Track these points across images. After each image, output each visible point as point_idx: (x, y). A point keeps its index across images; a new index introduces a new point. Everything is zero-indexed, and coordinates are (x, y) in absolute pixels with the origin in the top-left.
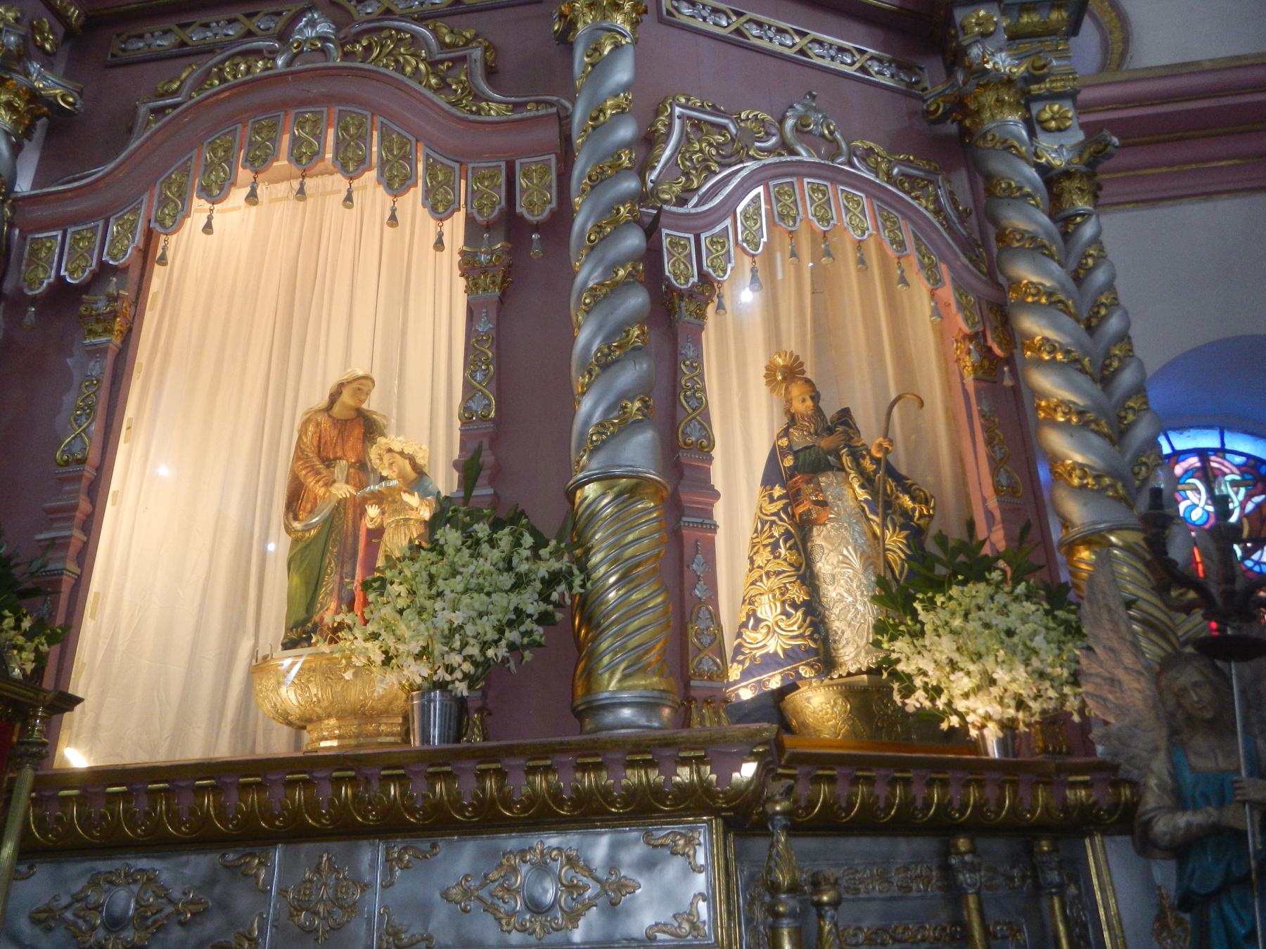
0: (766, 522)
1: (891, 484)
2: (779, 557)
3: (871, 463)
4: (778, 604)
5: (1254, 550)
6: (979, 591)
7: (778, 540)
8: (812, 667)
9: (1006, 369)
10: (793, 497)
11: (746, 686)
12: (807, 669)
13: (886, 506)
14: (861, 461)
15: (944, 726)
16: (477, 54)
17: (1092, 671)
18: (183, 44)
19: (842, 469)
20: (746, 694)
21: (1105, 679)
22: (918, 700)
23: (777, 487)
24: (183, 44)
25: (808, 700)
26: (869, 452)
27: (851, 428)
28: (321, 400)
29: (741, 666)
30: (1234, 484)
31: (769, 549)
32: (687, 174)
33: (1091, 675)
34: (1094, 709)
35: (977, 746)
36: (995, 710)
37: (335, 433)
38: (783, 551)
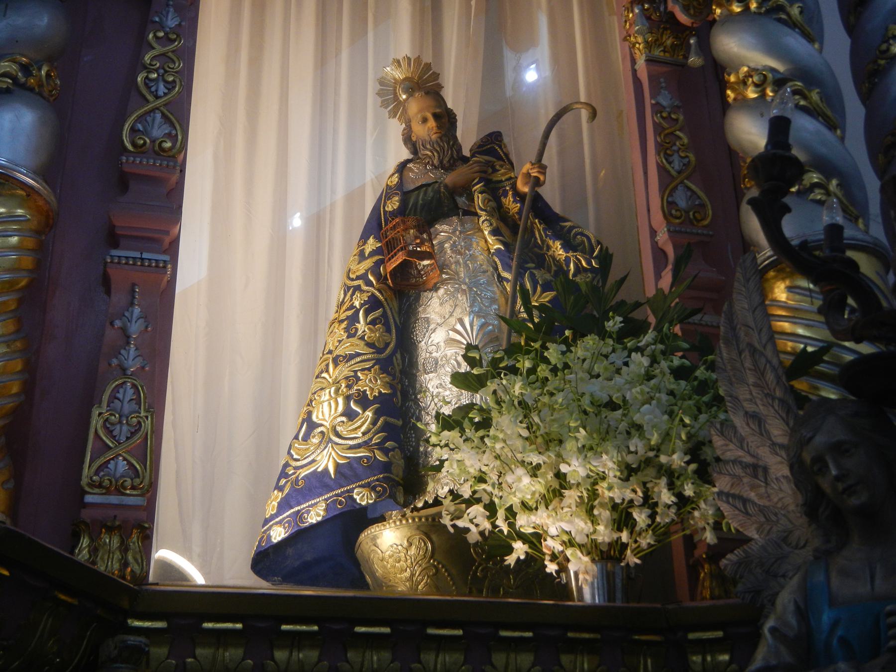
0: (349, 288)
2: (353, 335)
3: (515, 201)
4: (341, 400)
7: (358, 311)
8: (373, 489)
9: (692, 41)
11: (280, 523)
12: (365, 491)
14: (503, 200)
15: (511, 560)
17: (729, 455)
20: (278, 534)
21: (745, 466)
23: (371, 240)
25: (374, 539)
26: (514, 187)
27: (500, 158)
29: (280, 494)
31: (344, 325)
33: (726, 462)
34: (734, 522)
36: (580, 526)
38: (362, 326)
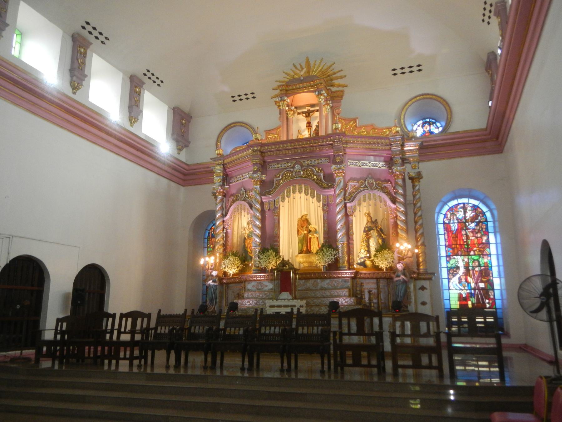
1: (381, 232)
5: (470, 224)
6: (385, 252)
10: (367, 235)
13: (379, 236)
16: (322, 174)
18: (278, 167)
19: (374, 230)
20: (359, 262)
22: (377, 264)
24: (278, 167)
28: (300, 217)
30: (469, 210)
32: (351, 194)
35: (383, 270)
36: (384, 266)
37: (303, 223)
38: (365, 243)
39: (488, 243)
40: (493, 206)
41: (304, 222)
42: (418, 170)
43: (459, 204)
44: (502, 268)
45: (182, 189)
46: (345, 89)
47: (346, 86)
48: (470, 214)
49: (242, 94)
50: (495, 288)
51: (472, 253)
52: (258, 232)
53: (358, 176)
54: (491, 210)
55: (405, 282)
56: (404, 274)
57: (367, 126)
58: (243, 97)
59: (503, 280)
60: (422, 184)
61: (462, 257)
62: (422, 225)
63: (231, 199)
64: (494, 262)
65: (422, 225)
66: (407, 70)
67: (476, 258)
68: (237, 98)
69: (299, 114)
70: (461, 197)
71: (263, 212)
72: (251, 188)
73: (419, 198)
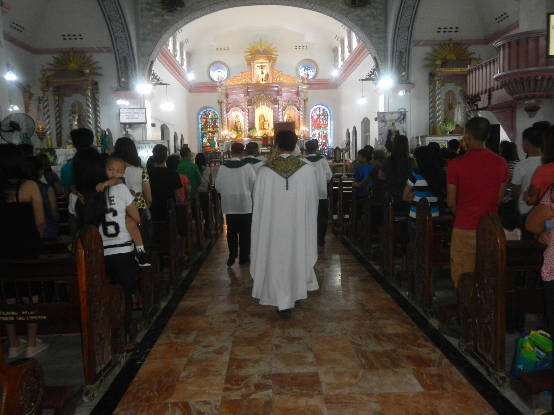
16: (273, 98)
28: (260, 114)
39: (327, 124)
40: (330, 109)
41: (262, 116)
42: (307, 97)
43: (317, 108)
44: (332, 135)
45: (190, 94)
46: (277, 57)
47: (278, 56)
48: (322, 112)
49: (223, 47)
50: (329, 142)
51: (321, 128)
52: (247, 121)
53: (286, 100)
54: (329, 111)
55: (303, 141)
56: (303, 138)
57: (286, 75)
58: (223, 49)
59: (332, 139)
60: (308, 103)
61: (318, 130)
62: (307, 119)
63: (230, 105)
64: (329, 132)
65: (307, 119)
66: (301, 47)
67: (323, 130)
68: (219, 49)
69: (257, 66)
70: (319, 105)
71: (248, 113)
72: (241, 101)
73: (307, 109)
